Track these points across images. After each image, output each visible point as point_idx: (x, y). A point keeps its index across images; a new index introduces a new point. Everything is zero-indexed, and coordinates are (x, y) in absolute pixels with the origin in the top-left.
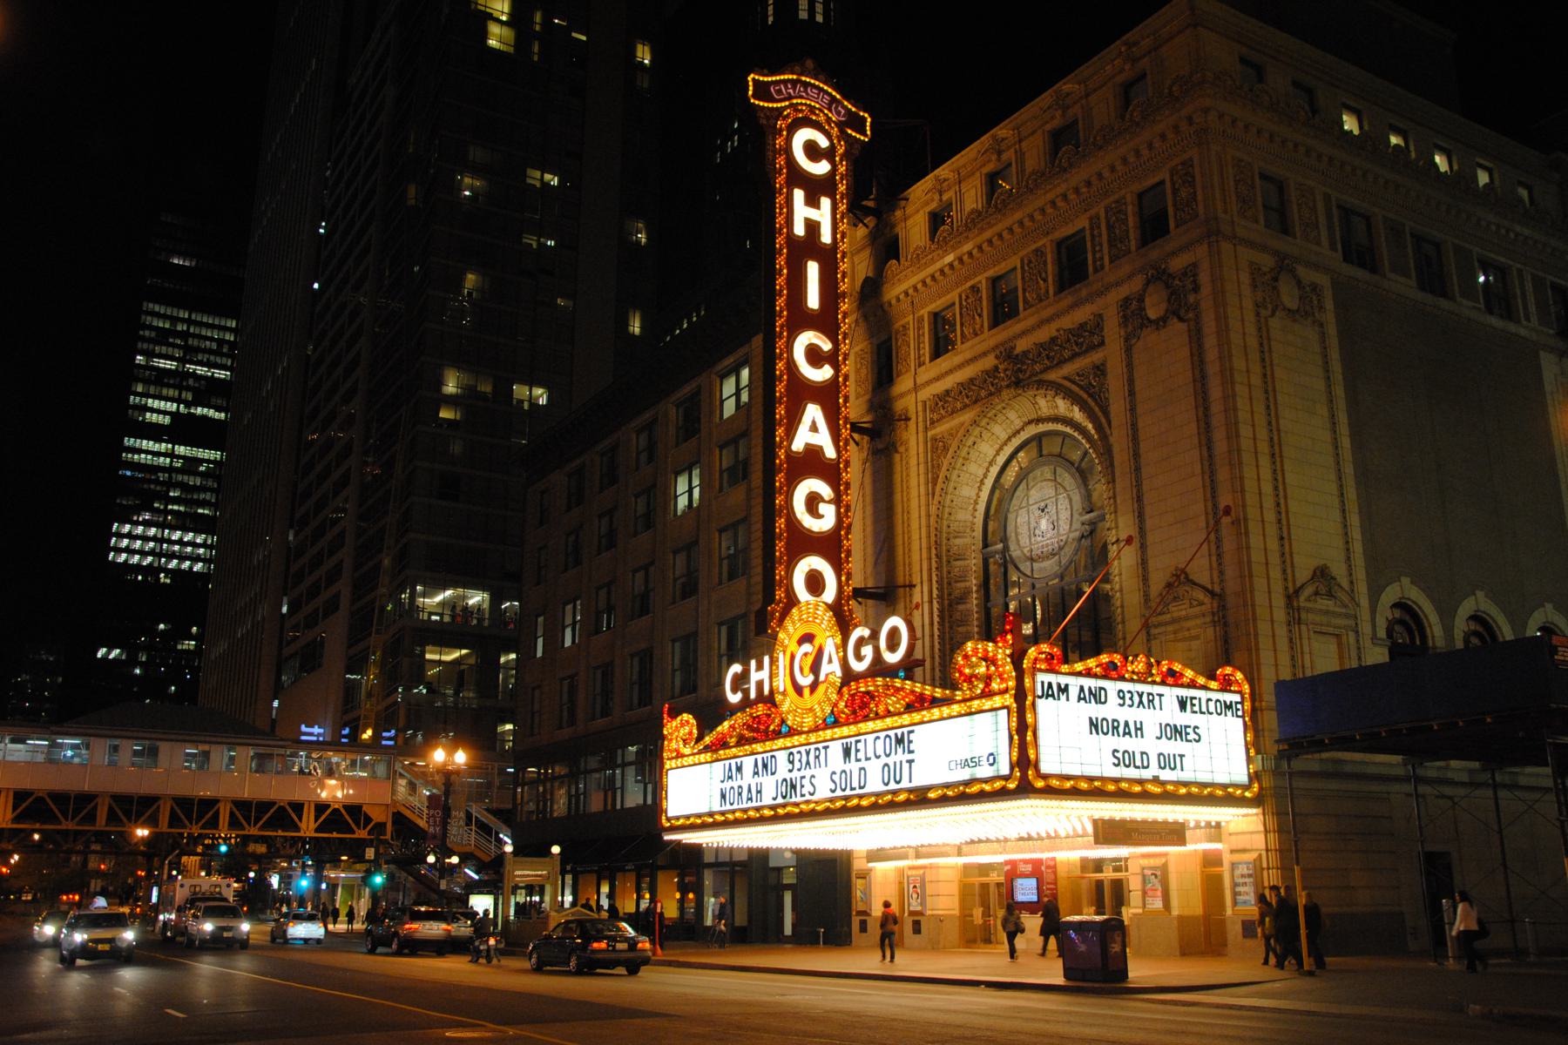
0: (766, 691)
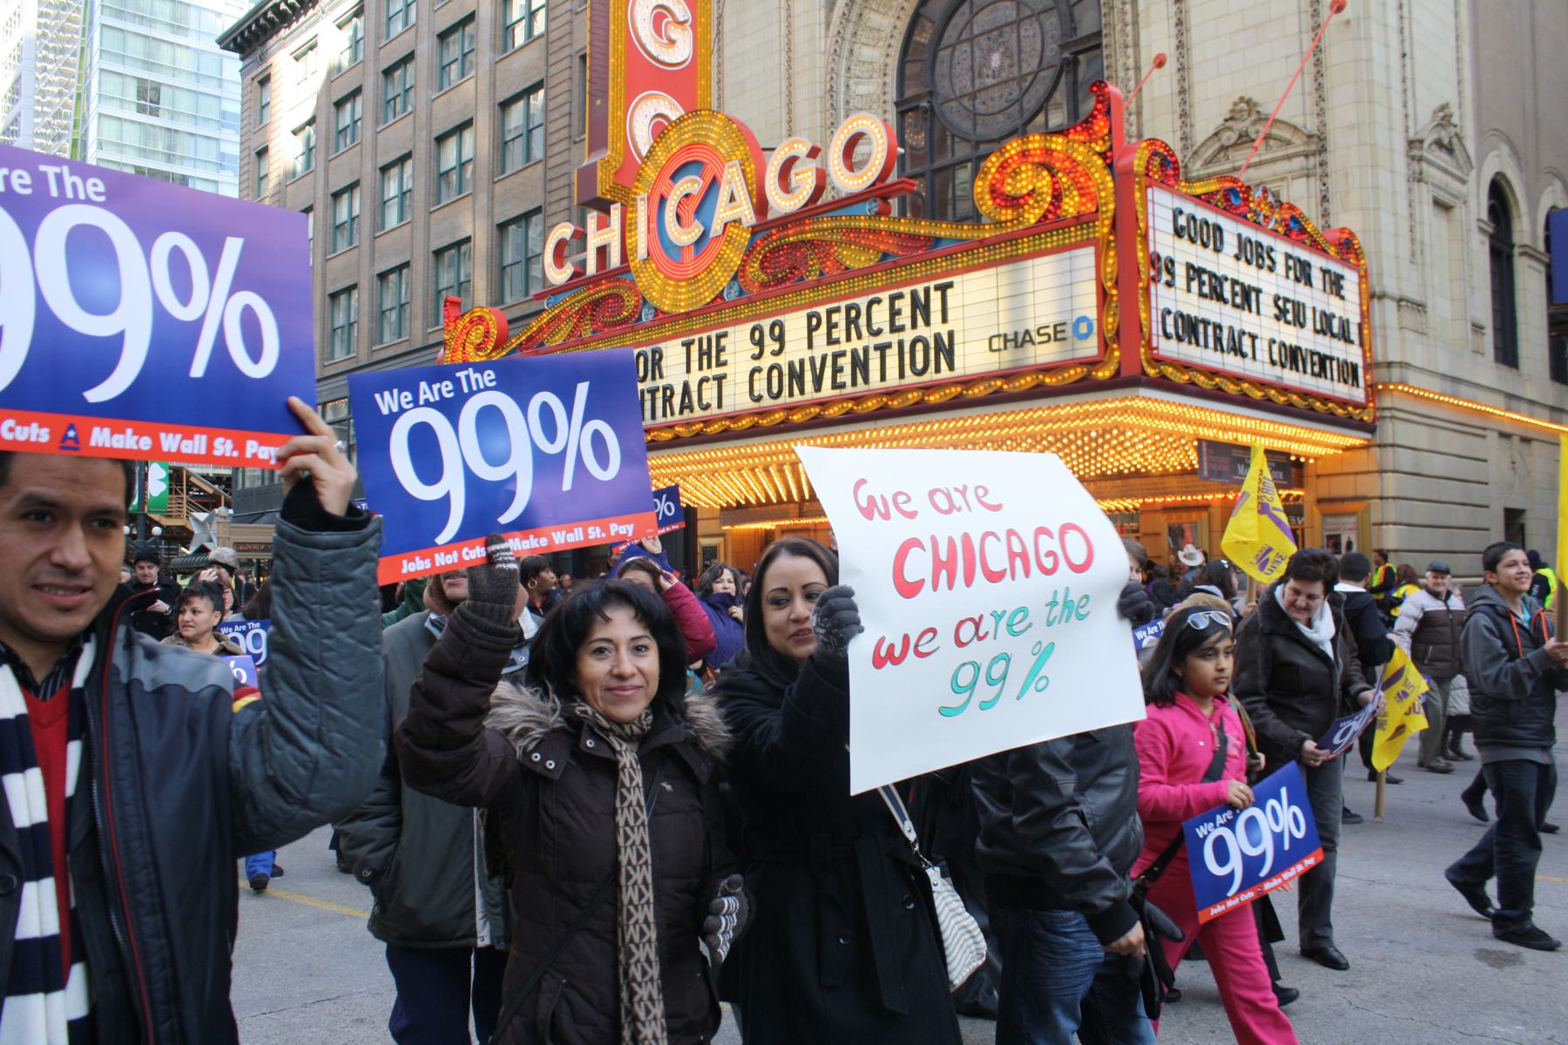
0: (615, 260)
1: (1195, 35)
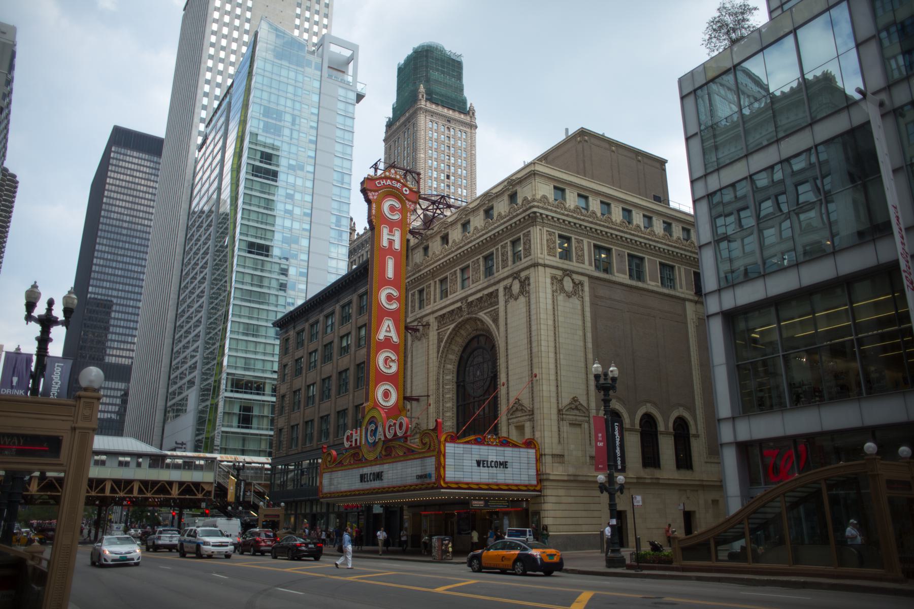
1: (510, 378)
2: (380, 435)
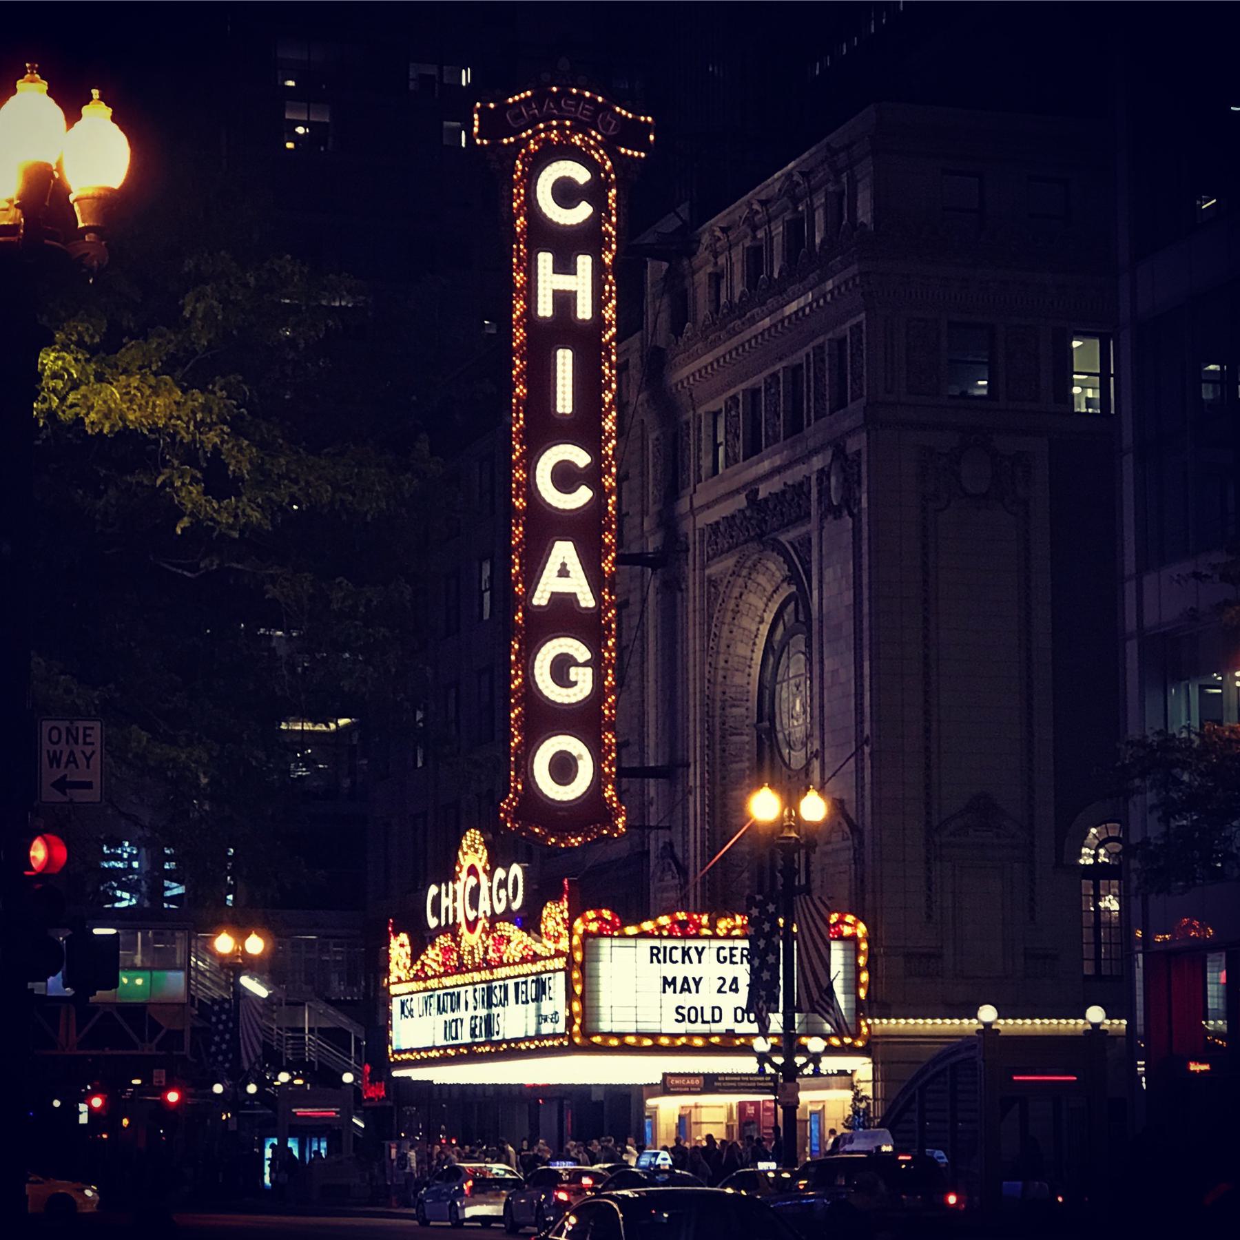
0: (451, 921)
2: (484, 905)
